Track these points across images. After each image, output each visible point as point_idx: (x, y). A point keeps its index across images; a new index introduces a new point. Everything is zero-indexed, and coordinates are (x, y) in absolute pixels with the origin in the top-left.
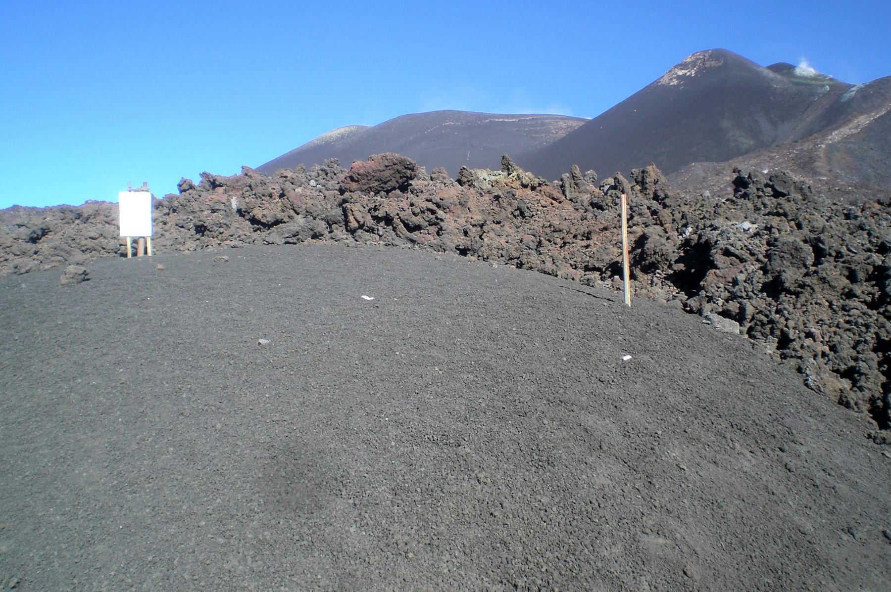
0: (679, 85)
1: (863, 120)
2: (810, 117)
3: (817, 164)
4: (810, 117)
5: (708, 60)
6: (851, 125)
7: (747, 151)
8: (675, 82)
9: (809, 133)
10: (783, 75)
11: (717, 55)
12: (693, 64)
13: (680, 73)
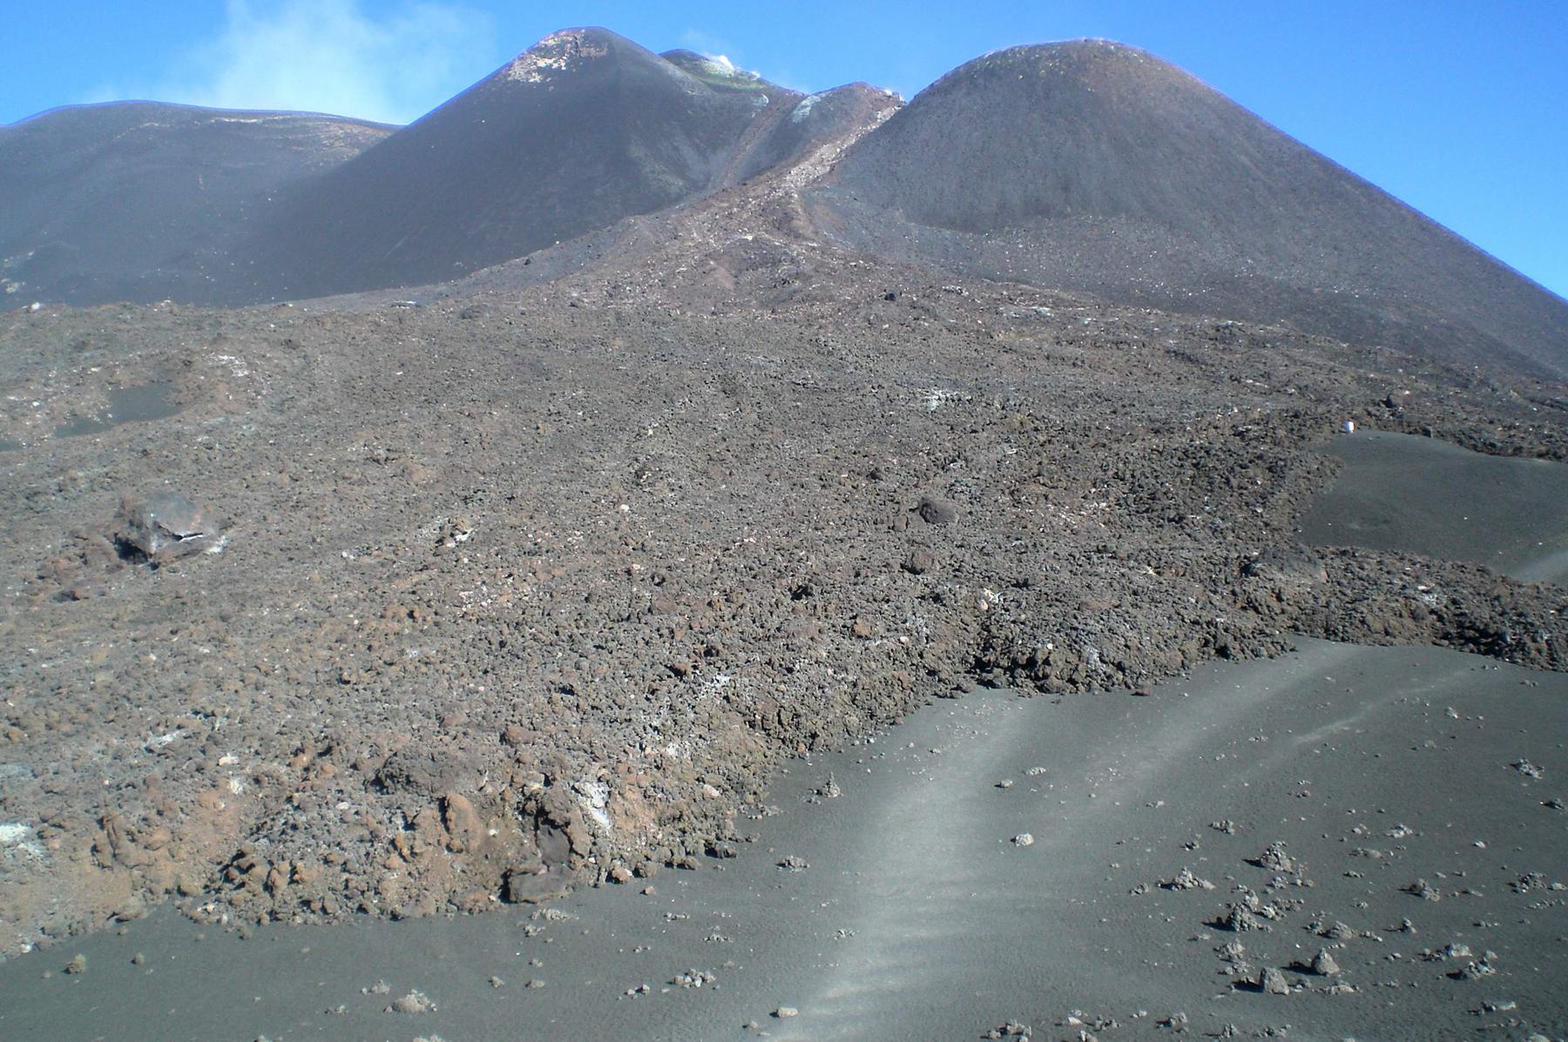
0: (543, 84)
1: (828, 152)
2: (750, 146)
3: (796, 223)
4: (750, 146)
5: (583, 45)
6: (812, 160)
7: (679, 198)
8: (537, 78)
9: (755, 171)
10: (686, 69)
11: (594, 37)
12: (560, 50)
13: (542, 63)
